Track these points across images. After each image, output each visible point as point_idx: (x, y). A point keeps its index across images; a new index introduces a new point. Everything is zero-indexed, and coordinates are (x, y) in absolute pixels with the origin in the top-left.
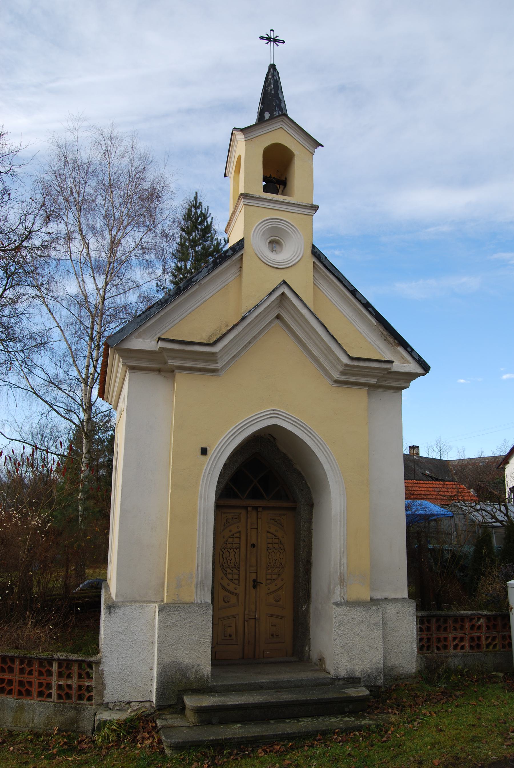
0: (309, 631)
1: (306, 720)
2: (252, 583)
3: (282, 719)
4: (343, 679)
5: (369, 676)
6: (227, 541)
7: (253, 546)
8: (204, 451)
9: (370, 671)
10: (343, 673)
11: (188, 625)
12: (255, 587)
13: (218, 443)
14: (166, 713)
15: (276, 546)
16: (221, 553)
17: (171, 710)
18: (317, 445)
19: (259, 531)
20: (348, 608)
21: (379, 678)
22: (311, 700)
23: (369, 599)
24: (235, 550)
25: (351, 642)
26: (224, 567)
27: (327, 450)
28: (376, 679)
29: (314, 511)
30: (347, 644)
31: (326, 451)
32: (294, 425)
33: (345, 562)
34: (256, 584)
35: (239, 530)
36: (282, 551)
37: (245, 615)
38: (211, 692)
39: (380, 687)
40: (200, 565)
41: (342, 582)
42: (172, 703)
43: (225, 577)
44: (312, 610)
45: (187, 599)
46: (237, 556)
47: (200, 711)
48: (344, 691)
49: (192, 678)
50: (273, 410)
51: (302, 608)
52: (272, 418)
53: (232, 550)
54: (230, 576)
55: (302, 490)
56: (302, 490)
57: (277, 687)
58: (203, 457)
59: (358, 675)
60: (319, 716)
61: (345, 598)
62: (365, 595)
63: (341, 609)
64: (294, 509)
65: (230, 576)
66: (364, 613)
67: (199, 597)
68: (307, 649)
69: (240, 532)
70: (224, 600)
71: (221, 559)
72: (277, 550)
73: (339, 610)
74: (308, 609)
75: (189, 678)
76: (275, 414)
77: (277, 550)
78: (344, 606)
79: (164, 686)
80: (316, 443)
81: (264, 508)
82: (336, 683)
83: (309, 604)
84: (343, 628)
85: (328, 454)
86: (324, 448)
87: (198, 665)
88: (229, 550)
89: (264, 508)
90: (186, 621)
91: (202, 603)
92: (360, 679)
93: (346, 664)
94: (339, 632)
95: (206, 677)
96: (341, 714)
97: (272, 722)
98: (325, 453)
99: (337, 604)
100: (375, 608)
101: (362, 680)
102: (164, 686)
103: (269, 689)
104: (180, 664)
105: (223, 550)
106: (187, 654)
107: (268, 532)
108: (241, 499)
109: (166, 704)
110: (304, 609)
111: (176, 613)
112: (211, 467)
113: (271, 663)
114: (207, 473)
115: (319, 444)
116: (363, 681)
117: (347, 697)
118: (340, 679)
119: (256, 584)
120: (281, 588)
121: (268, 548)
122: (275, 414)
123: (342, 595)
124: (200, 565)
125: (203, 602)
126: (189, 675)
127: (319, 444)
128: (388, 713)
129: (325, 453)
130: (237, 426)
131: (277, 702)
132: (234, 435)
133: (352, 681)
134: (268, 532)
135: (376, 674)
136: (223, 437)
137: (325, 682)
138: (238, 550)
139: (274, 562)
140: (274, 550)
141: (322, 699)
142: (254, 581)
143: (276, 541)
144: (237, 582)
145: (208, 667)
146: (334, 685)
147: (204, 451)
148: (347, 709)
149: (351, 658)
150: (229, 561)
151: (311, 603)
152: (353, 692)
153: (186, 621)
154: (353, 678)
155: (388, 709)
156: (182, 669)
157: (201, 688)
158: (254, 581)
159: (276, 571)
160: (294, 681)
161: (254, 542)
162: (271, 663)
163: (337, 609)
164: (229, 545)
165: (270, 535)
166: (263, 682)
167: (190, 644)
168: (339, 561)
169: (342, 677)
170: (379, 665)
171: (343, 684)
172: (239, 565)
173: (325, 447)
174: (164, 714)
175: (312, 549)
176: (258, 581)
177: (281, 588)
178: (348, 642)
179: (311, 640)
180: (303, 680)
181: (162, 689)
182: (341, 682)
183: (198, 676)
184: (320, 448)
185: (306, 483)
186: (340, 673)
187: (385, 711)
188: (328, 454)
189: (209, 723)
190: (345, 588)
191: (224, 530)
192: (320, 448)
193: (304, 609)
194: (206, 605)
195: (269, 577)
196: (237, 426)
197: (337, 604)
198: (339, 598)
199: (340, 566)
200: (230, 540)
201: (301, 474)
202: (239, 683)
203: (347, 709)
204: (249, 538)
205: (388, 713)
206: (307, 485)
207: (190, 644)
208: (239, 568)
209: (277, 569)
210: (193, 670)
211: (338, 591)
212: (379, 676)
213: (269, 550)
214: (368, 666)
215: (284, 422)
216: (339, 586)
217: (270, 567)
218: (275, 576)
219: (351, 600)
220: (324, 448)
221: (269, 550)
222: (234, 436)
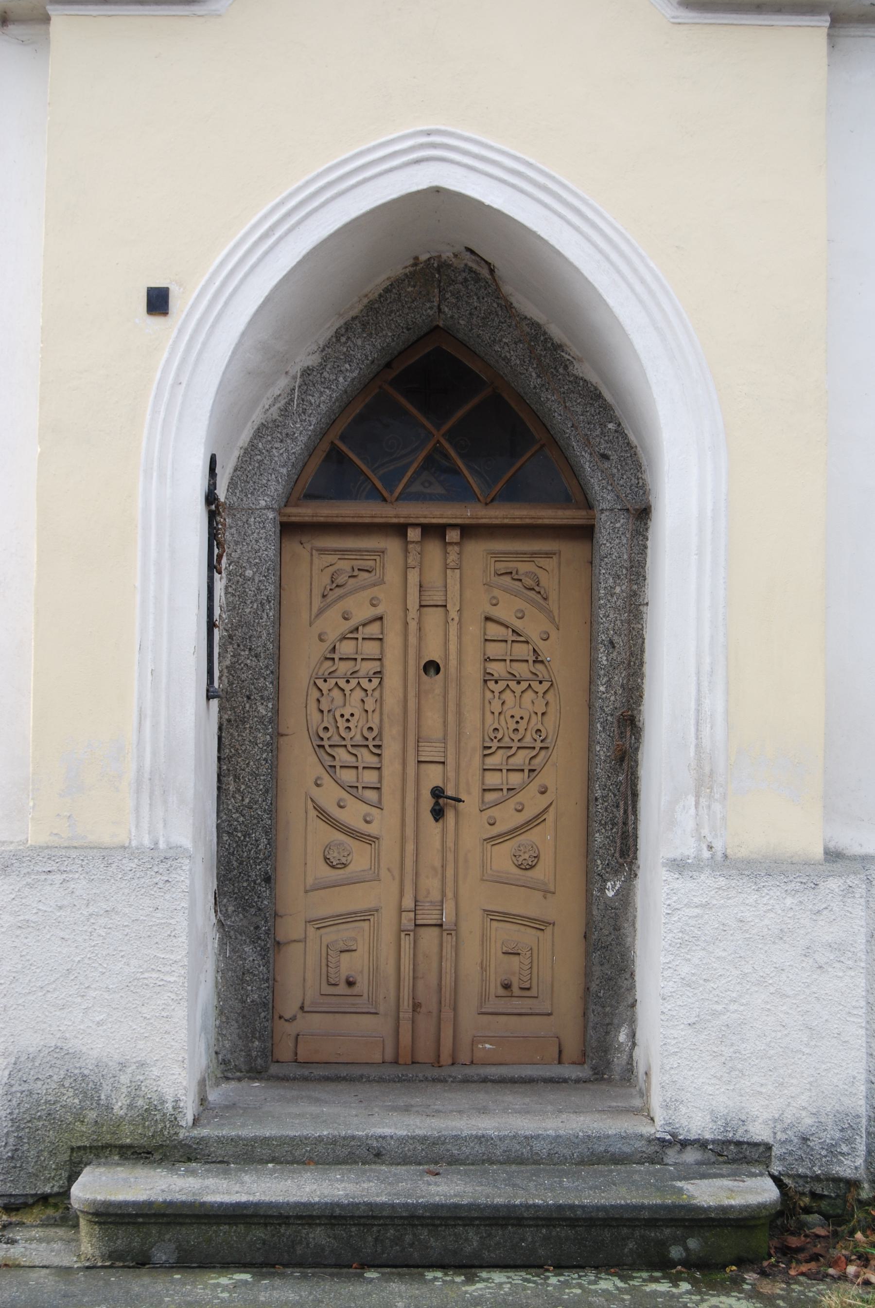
0: (632, 975)
1: (498, 1277)
2: (427, 802)
3: (418, 1267)
4: (702, 1144)
5: (805, 1139)
6: (334, 649)
7: (432, 667)
8: (158, 302)
9: (809, 1121)
10: (697, 1123)
11: (102, 921)
12: (438, 813)
13: (211, 269)
14: (28, 1220)
15: (521, 670)
16: (316, 694)
17: (50, 1212)
18: (607, 258)
19: (453, 614)
20: (722, 881)
21: (845, 1148)
22: (528, 1207)
23: (818, 852)
24: (365, 683)
25: (733, 1007)
26: (326, 743)
27: (649, 278)
28: (832, 1151)
29: (650, 535)
30: (715, 1014)
31: (643, 281)
32: (513, 186)
33: (720, 708)
34: (441, 804)
35: (378, 611)
36: (541, 689)
37: (401, 911)
38: (189, 1160)
39: (853, 1184)
40: (149, 712)
41: (704, 782)
42: (48, 1190)
43: (327, 780)
44: (639, 899)
45: (106, 833)
46: (370, 705)
47: (108, 1216)
48: (679, 1184)
49: (119, 1107)
50: (429, 133)
51: (602, 890)
52: (424, 165)
53: (353, 682)
54: (348, 776)
55: (605, 457)
56: (605, 457)
57: (433, 1156)
58: (157, 322)
59: (759, 1132)
60: (560, 1267)
61: (718, 845)
62: (807, 839)
63: (691, 885)
64: (585, 533)
65: (348, 776)
66: (789, 901)
67: (145, 825)
68: (622, 1037)
69: (381, 618)
70: (326, 859)
71: (315, 716)
72: (524, 685)
73: (683, 885)
74: (626, 898)
75: (109, 1108)
76: (431, 147)
77: (524, 685)
78: (707, 871)
79: (18, 1129)
80: (601, 251)
81: (468, 531)
82: (672, 1155)
83: (633, 875)
84: (702, 954)
85: (651, 292)
86: (635, 271)
87: (142, 1065)
88: (342, 683)
89: (468, 531)
90: (91, 909)
91: (155, 848)
92: (768, 1147)
93: (710, 1090)
94: (685, 970)
95: (169, 1106)
96: (651, 1266)
97: (371, 1274)
98: (639, 288)
99: (679, 866)
100: (834, 884)
101: (776, 1151)
102: (18, 1129)
103: (405, 1161)
104: (75, 1055)
105: (320, 683)
106: (98, 1024)
107: (488, 619)
108: (385, 500)
109: (29, 1191)
110: (610, 894)
111: (58, 878)
112: (184, 360)
113: (485, 1080)
114: (170, 381)
115: (614, 256)
116: (782, 1158)
117: (682, 1207)
118: (685, 1144)
119: (441, 804)
120: (537, 820)
121: (488, 678)
122: (434, 146)
123: (705, 831)
124: (149, 712)
125: (162, 845)
126: (108, 1097)
127: (614, 256)
128: (843, 1277)
129: (639, 288)
130: (282, 203)
131: (393, 1206)
132: (271, 237)
133: (735, 1153)
134: (488, 619)
135: (832, 1134)
136: (231, 244)
137: (627, 1149)
138: (376, 682)
139: (513, 726)
140: (513, 684)
141: (572, 1207)
142: (437, 793)
143: (522, 651)
144: (371, 795)
145: (177, 1070)
146: (661, 1162)
147: (158, 302)
148: (676, 1252)
149: (733, 1069)
150: (342, 724)
151: (640, 873)
152: (711, 1192)
153: (91, 909)
154: (739, 1144)
155: (849, 1261)
156: (84, 1076)
157: (153, 1145)
158: (437, 793)
159: (521, 758)
160: (501, 1139)
161: (435, 655)
162: (485, 1080)
163: (676, 885)
164: (344, 668)
165: (494, 630)
166: (384, 1138)
167: (108, 989)
168: (693, 705)
169: (692, 1136)
170: (847, 1101)
171: (699, 1163)
172: (380, 734)
173: (642, 269)
174: (21, 1224)
175: (642, 676)
176: (450, 792)
177: (537, 820)
178: (719, 1008)
179: (639, 1007)
180: (537, 1137)
181: (11, 1140)
182: (691, 1156)
183: (140, 1102)
184: (619, 272)
185: (620, 431)
186: (685, 1123)
187: (831, 1271)
188: (651, 292)
189: (141, 1262)
190: (717, 807)
191: (321, 612)
192: (619, 272)
193: (610, 894)
194: (169, 858)
195: (493, 780)
196: (282, 203)
197: (679, 866)
198: (692, 842)
199: (697, 723)
200: (347, 648)
201: (599, 396)
202: (292, 1133)
203: (676, 1252)
204: (413, 640)
205: (843, 1277)
206: (625, 437)
207: (108, 989)
208: (379, 747)
209: (522, 753)
210: (124, 1079)
211: (686, 817)
212: (849, 1141)
213: (491, 684)
214: (803, 1100)
215: (473, 176)
216: (691, 800)
217: (495, 744)
218: (515, 779)
219: (743, 853)
220: (635, 271)
221: (491, 684)
222: (273, 239)
